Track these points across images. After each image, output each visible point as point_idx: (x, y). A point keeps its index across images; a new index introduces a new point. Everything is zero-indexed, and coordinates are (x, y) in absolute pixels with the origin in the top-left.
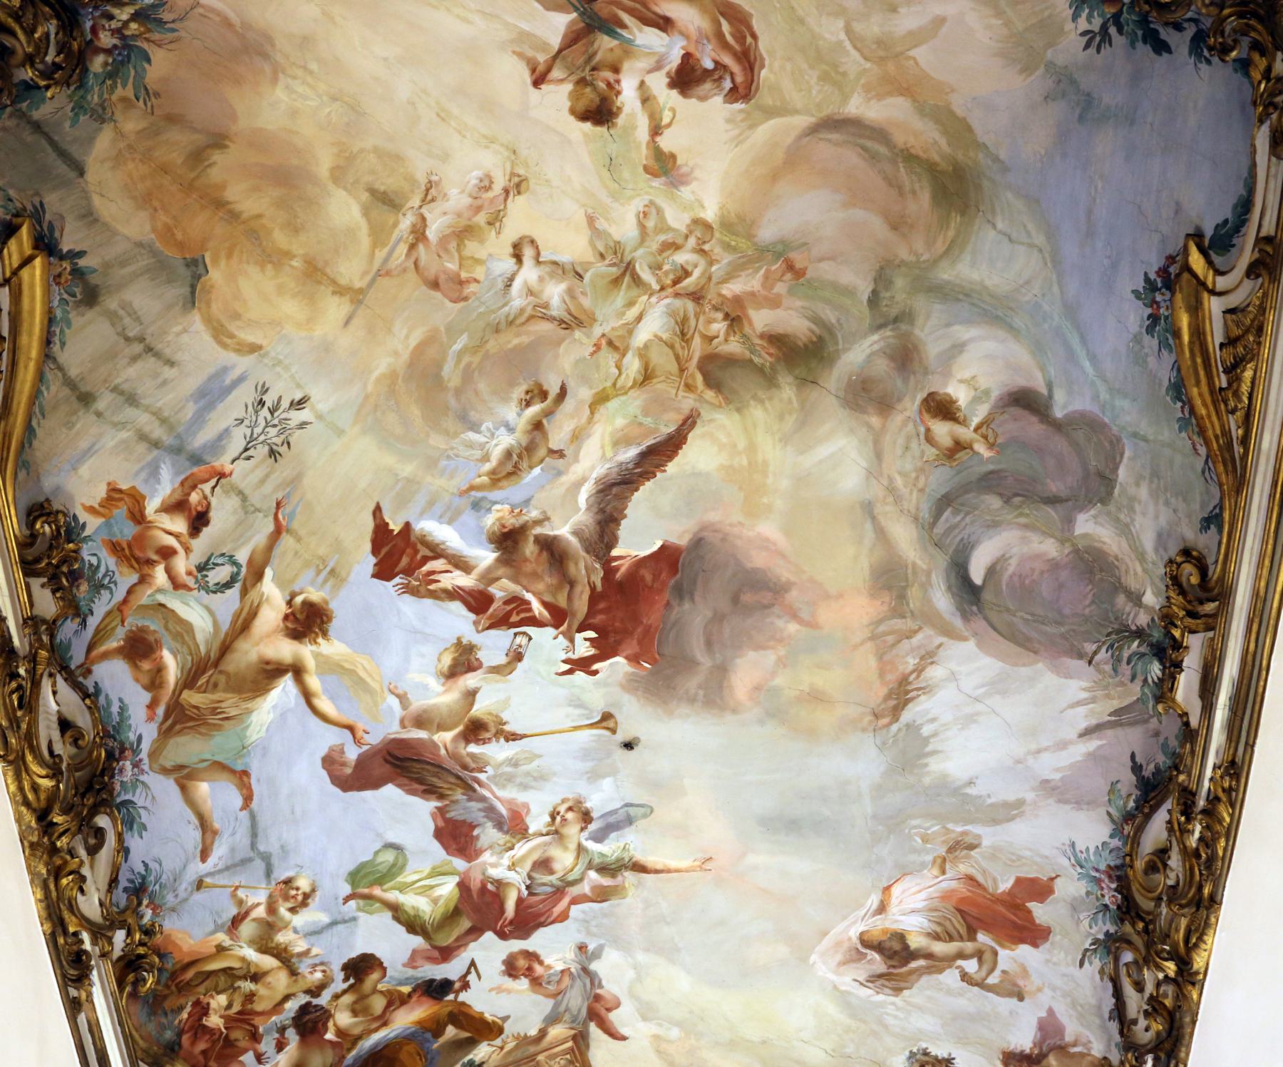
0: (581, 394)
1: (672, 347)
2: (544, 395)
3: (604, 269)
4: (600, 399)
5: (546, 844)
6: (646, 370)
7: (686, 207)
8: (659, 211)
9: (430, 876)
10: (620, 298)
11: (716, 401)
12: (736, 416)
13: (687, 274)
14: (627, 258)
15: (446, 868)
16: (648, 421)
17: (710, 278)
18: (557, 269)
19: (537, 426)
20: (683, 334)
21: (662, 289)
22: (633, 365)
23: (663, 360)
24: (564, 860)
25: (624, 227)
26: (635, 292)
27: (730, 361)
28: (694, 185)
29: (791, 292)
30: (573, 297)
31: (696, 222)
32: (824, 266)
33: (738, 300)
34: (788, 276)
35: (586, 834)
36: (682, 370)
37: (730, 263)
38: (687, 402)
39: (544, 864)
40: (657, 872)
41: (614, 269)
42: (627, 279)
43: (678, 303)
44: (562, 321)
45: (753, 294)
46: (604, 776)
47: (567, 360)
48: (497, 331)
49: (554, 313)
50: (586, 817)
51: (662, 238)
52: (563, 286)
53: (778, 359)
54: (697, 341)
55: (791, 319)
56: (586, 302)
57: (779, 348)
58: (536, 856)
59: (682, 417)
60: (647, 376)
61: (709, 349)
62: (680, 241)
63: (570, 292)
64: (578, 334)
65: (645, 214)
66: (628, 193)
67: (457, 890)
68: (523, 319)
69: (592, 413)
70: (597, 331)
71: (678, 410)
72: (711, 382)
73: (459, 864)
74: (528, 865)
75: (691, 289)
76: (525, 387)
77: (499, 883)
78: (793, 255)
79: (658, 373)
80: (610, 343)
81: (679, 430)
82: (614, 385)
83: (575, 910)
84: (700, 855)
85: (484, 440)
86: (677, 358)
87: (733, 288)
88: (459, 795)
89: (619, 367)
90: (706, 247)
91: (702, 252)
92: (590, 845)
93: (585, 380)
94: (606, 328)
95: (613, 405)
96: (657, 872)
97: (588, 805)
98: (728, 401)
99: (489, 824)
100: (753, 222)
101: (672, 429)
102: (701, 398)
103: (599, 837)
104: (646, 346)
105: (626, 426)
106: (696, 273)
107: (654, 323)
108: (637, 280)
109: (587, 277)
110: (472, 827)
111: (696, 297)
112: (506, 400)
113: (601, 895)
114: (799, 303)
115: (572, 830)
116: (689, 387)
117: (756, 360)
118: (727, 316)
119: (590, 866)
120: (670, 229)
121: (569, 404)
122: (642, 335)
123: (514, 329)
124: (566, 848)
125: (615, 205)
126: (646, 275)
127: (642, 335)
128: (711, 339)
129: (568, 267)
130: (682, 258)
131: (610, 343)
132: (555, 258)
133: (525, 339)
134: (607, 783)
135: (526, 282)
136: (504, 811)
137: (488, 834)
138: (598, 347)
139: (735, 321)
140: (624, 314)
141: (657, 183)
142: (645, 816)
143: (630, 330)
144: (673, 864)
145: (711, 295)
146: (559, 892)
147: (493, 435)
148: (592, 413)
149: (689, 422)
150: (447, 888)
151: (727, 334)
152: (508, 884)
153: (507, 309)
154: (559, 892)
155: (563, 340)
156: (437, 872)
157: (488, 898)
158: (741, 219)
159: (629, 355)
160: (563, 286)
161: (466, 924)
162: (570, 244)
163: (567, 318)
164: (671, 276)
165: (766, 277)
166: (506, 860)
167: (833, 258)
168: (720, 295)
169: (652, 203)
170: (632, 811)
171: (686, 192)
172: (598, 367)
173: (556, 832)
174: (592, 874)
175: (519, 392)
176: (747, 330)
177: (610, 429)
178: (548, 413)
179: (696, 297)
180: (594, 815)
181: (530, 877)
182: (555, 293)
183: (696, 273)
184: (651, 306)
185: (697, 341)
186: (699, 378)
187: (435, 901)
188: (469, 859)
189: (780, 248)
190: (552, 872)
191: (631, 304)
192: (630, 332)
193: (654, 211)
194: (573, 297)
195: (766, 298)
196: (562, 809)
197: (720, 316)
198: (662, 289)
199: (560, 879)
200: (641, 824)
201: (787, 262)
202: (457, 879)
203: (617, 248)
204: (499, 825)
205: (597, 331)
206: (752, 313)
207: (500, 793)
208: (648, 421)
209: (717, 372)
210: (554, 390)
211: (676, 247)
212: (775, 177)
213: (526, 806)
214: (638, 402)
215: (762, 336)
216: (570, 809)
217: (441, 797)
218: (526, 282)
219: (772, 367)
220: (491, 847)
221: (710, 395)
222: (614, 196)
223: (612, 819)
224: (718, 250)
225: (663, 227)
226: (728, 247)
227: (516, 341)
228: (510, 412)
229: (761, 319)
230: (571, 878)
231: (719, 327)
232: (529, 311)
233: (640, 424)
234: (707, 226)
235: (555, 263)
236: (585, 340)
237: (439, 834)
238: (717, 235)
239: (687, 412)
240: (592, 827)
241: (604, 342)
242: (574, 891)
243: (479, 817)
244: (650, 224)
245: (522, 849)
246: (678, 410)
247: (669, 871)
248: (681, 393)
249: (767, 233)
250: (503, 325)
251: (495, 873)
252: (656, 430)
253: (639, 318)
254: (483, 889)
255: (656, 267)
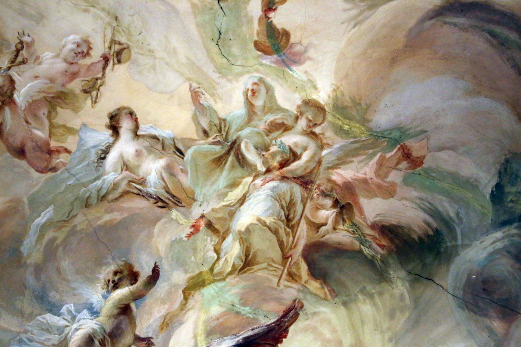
0: (175, 278)
1: (276, 232)
2: (134, 277)
3: (208, 147)
4: (196, 284)
6: (247, 256)
7: (297, 88)
8: (269, 90)
10: (223, 178)
11: (320, 293)
12: (342, 310)
13: (296, 157)
14: (232, 137)
16: (246, 310)
17: (319, 163)
18: (157, 144)
19: (124, 310)
20: (288, 219)
21: (268, 171)
22: (233, 250)
23: (266, 246)
25: (230, 105)
26: (239, 172)
27: (339, 251)
28: (307, 66)
29: (406, 181)
30: (172, 175)
31: (308, 103)
32: (444, 155)
33: (349, 187)
34: (404, 164)
36: (285, 258)
37: (340, 149)
38: (290, 293)
41: (218, 148)
42: (231, 158)
43: (284, 186)
44: (158, 199)
45: (365, 181)
47: (162, 241)
48: (87, 205)
49: (151, 190)
51: (270, 118)
52: (162, 162)
53: (390, 252)
54: (303, 229)
55: (405, 210)
56: (186, 181)
57: (392, 240)
59: (281, 309)
60: (248, 262)
61: (316, 237)
62: (289, 122)
63: (169, 169)
64: (175, 213)
65: (254, 92)
66: (237, 69)
68: (117, 194)
69: (186, 299)
70: (196, 211)
71: (279, 300)
72: (317, 273)
75: (299, 173)
76: (113, 268)
78: (409, 143)
79: (259, 259)
80: (210, 225)
81: (279, 322)
82: (212, 269)
85: (63, 323)
86: (281, 244)
87: (344, 174)
89: (217, 251)
90: (317, 130)
91: (312, 135)
93: (181, 263)
94: (206, 209)
95: (209, 291)
98: (334, 293)
100: (368, 107)
101: (272, 320)
102: (305, 289)
104: (248, 230)
105: (223, 315)
106: (305, 157)
107: (258, 206)
108: (242, 161)
109: (189, 154)
111: (305, 181)
112: (91, 280)
114: (415, 194)
116: (292, 277)
117: (366, 251)
118: (336, 203)
120: (280, 109)
121: (161, 287)
122: (245, 219)
123: (105, 204)
125: (223, 81)
126: (251, 156)
127: (245, 219)
128: (318, 227)
129: (168, 143)
130: (292, 139)
131: (210, 225)
132: (154, 132)
133: (117, 216)
135: (121, 157)
138: (196, 228)
139: (344, 208)
140: (226, 195)
141: (267, 60)
143: (232, 212)
145: (320, 180)
147: (74, 318)
148: (186, 299)
149: (291, 314)
151: (336, 222)
153: (99, 182)
155: (158, 219)
158: (356, 102)
159: (229, 239)
160: (162, 162)
162: (173, 119)
163: (164, 196)
164: (279, 158)
165: (380, 164)
167: (452, 148)
168: (330, 180)
169: (261, 81)
171: (298, 72)
172: (195, 250)
175: (106, 272)
176: (357, 218)
177: (203, 317)
178: (138, 297)
179: (305, 181)
182: (153, 169)
183: (305, 157)
184: (256, 188)
185: (303, 227)
186: (304, 267)
189: (396, 134)
191: (233, 185)
192: (232, 215)
193: (263, 90)
194: (172, 175)
195: (379, 187)
197: (329, 202)
198: (268, 171)
201: (403, 149)
203: (222, 126)
205: (196, 211)
206: (364, 202)
208: (246, 310)
209: (323, 262)
210: (145, 272)
211: (284, 128)
212: (394, 60)
214: (236, 290)
215: (373, 226)
218: (121, 157)
219: (384, 260)
221: (314, 285)
222: (221, 71)
224: (329, 134)
225: (272, 106)
226: (340, 131)
227: (107, 218)
228: (95, 295)
229: (372, 208)
231: (327, 214)
232: (123, 186)
233: (238, 313)
234: (319, 109)
235: (155, 138)
236: (182, 220)
238: (329, 118)
239: (289, 303)
241: (202, 223)
244: (259, 103)
246: (279, 300)
248: (283, 282)
249: (383, 118)
250: (94, 200)
252: (255, 320)
253: (242, 201)
255: (262, 148)
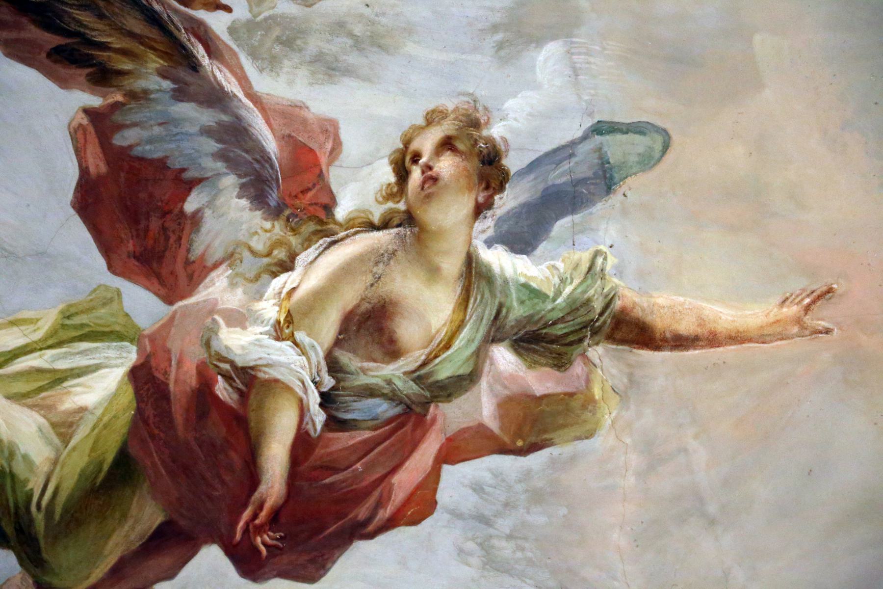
5: (383, 257)
9: (57, 339)
15: (102, 316)
24: (428, 308)
35: (487, 225)
39: (371, 325)
40: (680, 342)
46: (539, 42)
50: (490, 171)
58: (350, 296)
67: (128, 395)
73: (141, 304)
74: (329, 325)
77: (250, 380)
83: (456, 482)
84: (797, 284)
88: (150, 76)
92: (499, 260)
96: (680, 342)
97: (496, 131)
99: (230, 181)
103: (522, 238)
110: (186, 185)
113: (530, 427)
115: (450, 213)
119: (495, 335)
124: (433, 272)
134: (548, 58)
136: (271, 145)
137: (227, 215)
142: (648, 162)
144: (725, 315)
146: (411, 417)
150: (101, 385)
152: (274, 385)
154: (411, 418)
156: (80, 328)
157: (216, 430)
161: (145, 514)
166: (270, 310)
170: (616, 147)
173: (409, 219)
174: (504, 358)
180: (513, 163)
181: (334, 367)
187: (63, 428)
188: (170, 293)
190: (392, 350)
196: (426, 144)
199: (418, 376)
200: (635, 188)
202: (130, 356)
204: (258, 188)
207: (264, 84)
213: (330, 130)
216: (447, 145)
217: (103, 77)
220: (230, 258)
223: (558, 176)
230: (444, 371)
237: (89, 201)
240: (507, 201)
242: (452, 415)
243: (203, 154)
245: (317, 268)
247: (713, 340)
251: (242, 343)
254: (204, 392)
